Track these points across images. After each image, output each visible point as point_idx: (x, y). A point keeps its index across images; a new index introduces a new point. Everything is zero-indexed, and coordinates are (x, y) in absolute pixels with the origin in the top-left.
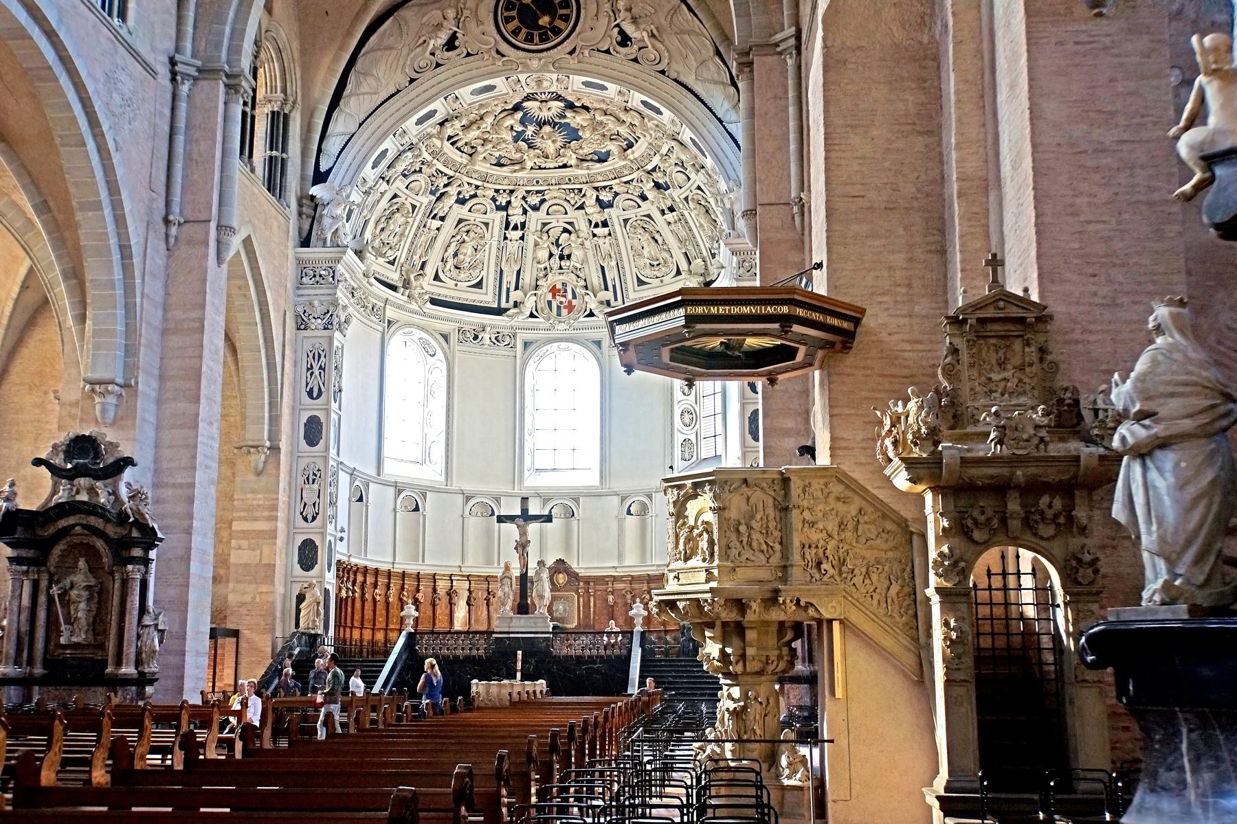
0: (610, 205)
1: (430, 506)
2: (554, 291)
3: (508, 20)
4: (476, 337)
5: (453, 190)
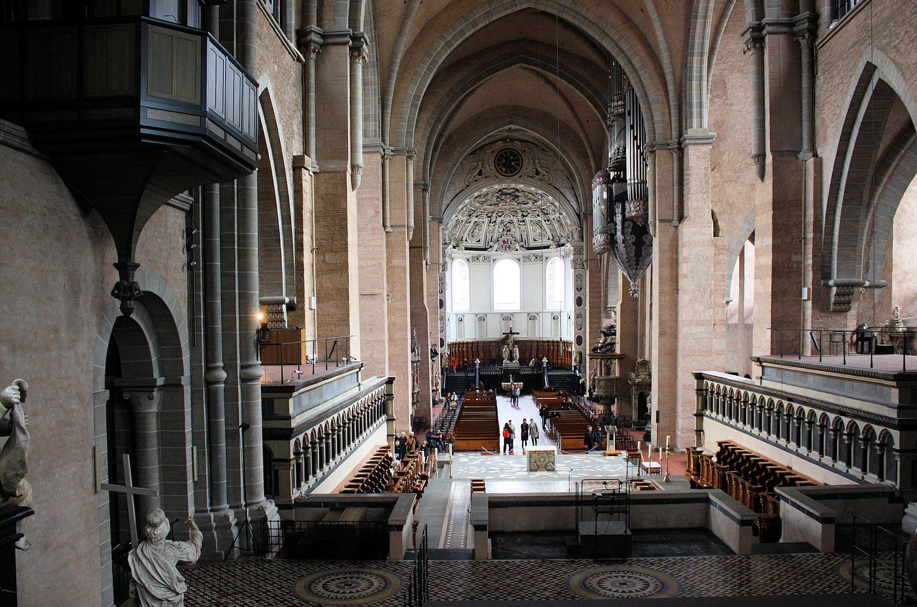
0: (526, 216)
1: (465, 320)
2: (504, 242)
3: (499, 165)
4: (477, 259)
5: (475, 215)
